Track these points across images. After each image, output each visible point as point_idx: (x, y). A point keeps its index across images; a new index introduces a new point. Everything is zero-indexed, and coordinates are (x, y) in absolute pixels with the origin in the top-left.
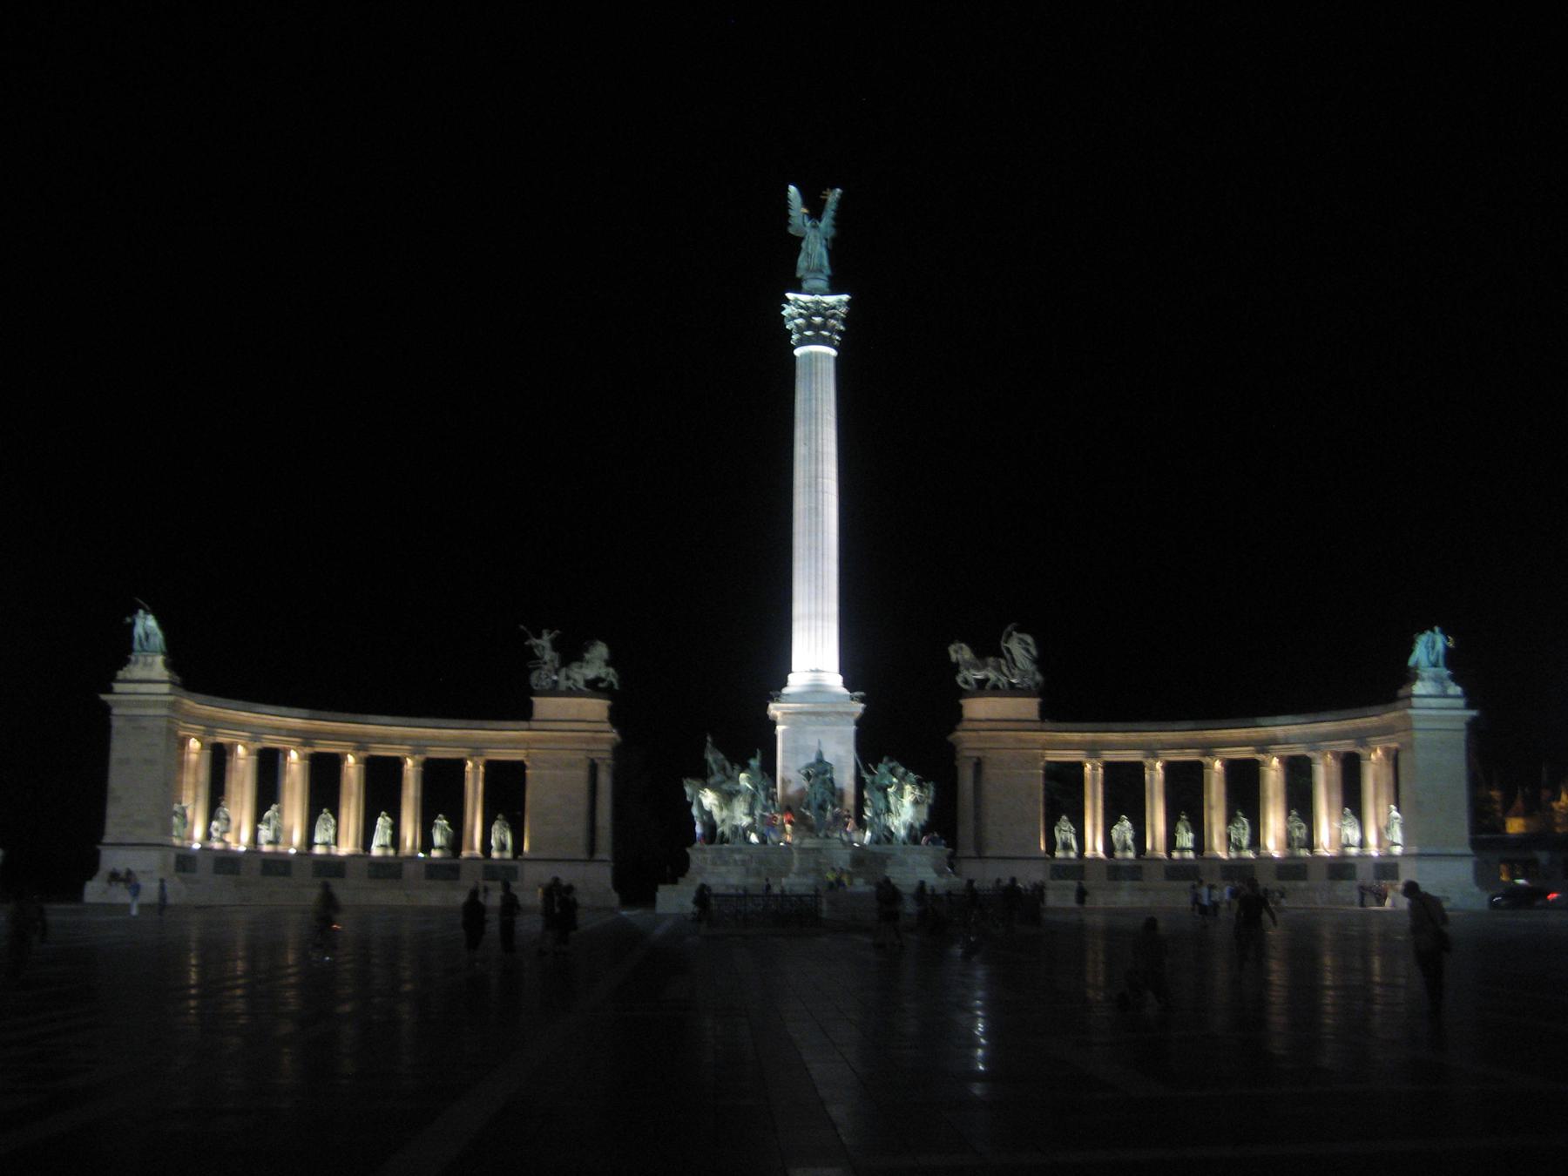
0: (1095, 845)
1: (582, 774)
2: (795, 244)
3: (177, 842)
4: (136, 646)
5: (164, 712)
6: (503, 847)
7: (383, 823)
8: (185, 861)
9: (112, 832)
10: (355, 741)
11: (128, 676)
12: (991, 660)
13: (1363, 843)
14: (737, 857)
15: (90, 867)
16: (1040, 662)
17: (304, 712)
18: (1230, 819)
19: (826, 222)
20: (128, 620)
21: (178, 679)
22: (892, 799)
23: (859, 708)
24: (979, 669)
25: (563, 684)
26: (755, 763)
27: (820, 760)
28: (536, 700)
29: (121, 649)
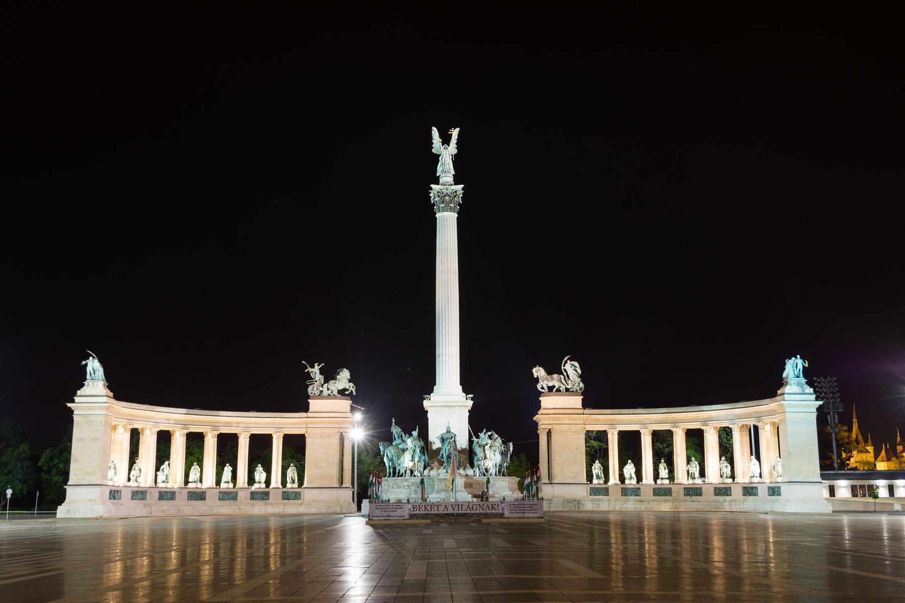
0: (614, 479)
2: (436, 158)
3: (110, 483)
4: (88, 376)
5: (104, 412)
6: (293, 482)
7: (228, 470)
8: (114, 494)
9: (72, 479)
10: (214, 423)
11: (83, 394)
12: (555, 376)
13: (761, 476)
14: (405, 484)
15: (61, 498)
16: (582, 377)
17: (184, 411)
18: (689, 461)
19: (453, 148)
20: (84, 363)
21: (111, 394)
22: (487, 452)
23: (470, 403)
24: (547, 380)
25: (326, 393)
26: (415, 433)
27: (448, 432)
29: (79, 378)
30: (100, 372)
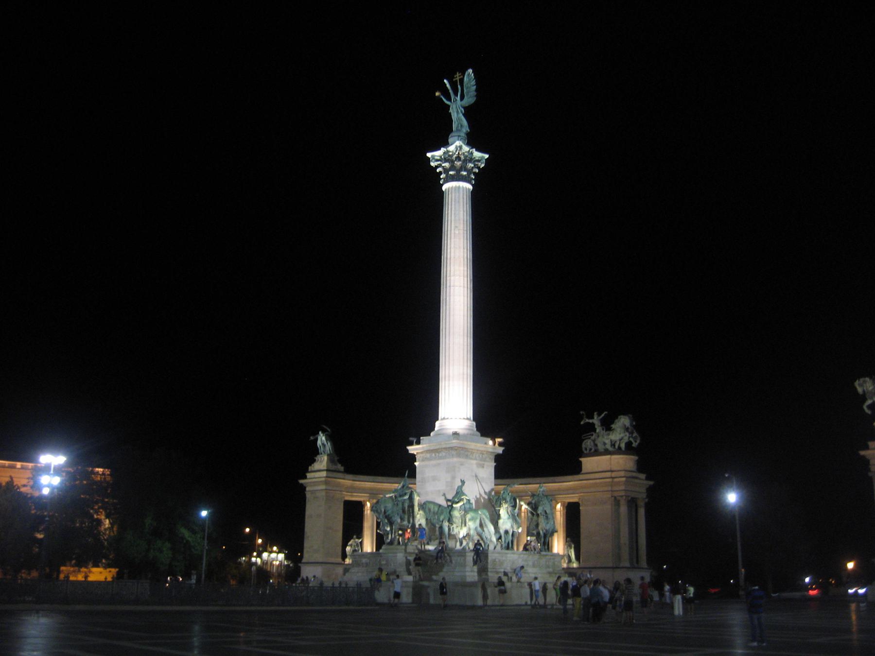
1: (608, 507)
5: (323, 487)
20: (312, 438)
25: (601, 447)
28: (583, 460)
29: (313, 453)
30: (329, 446)
